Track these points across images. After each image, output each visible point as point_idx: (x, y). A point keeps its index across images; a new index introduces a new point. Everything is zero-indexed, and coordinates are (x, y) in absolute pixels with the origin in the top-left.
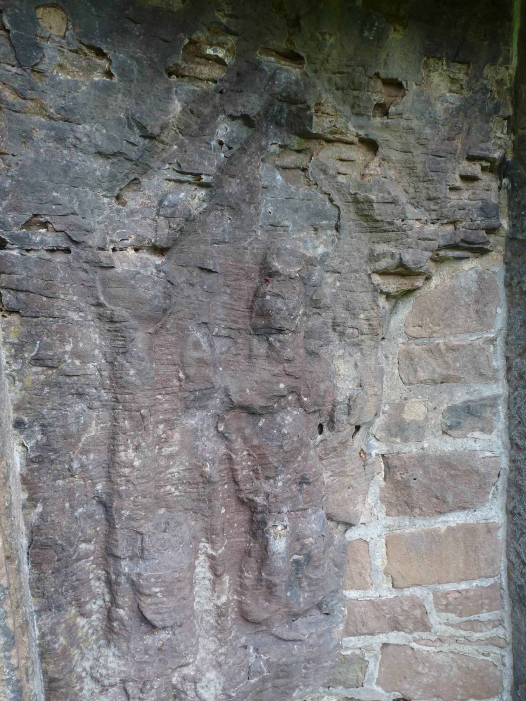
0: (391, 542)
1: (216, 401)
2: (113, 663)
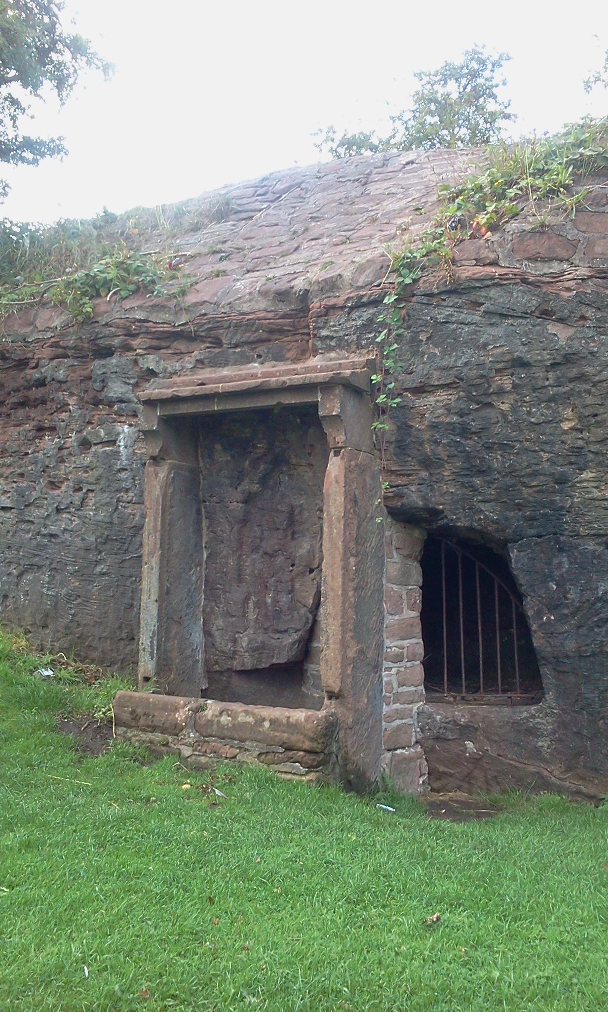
1: (261, 551)
2: (220, 622)
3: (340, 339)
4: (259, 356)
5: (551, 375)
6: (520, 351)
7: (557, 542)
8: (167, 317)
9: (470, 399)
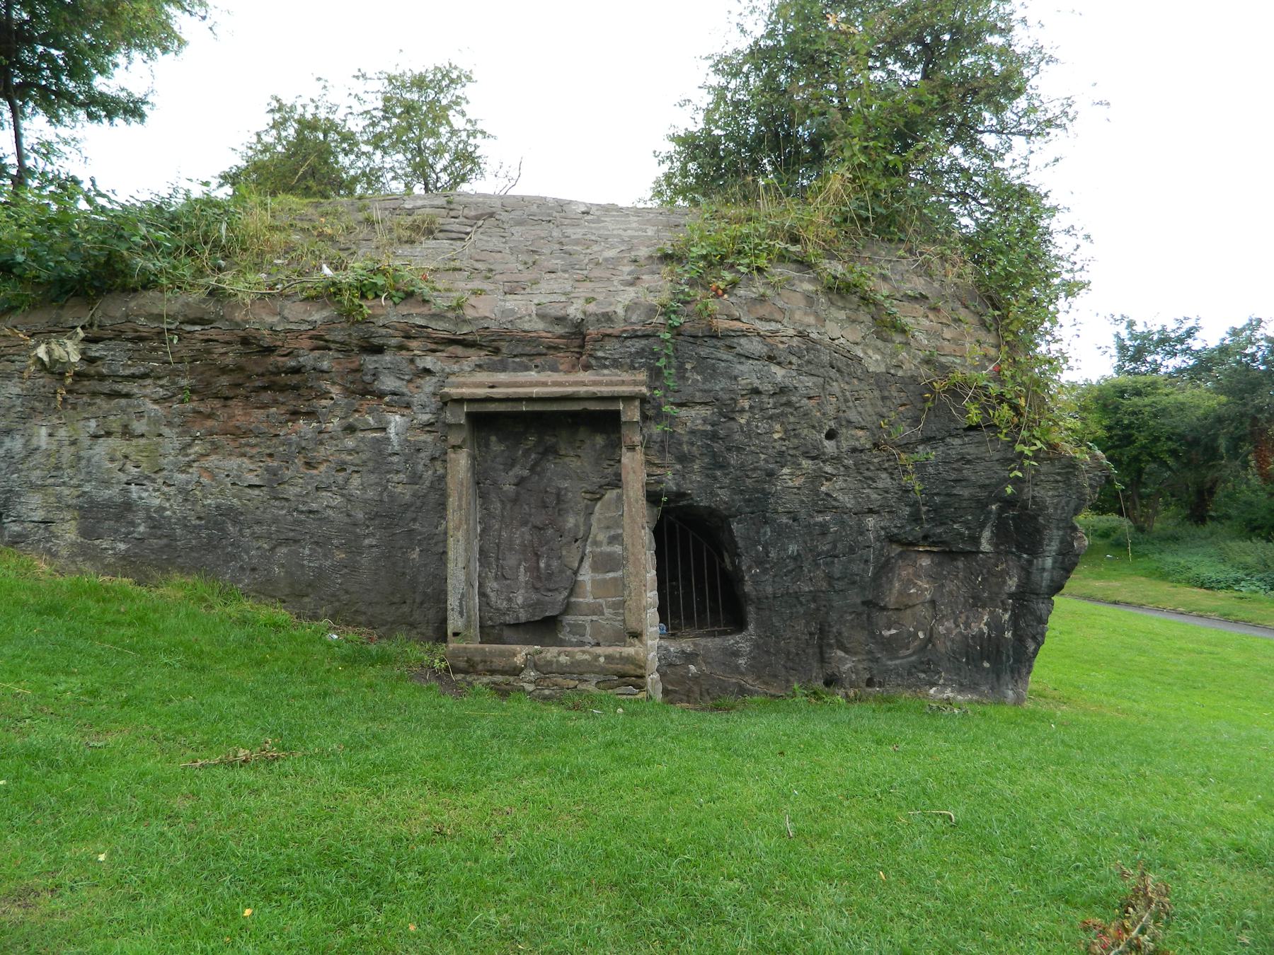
0: (593, 581)
2: (495, 585)
3: (615, 360)
4: (536, 366)
5: (771, 401)
6: (757, 383)
7: (764, 517)
8: (446, 326)
9: (721, 414)
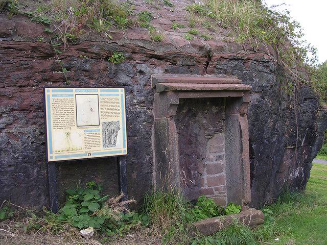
3: (225, 70)
